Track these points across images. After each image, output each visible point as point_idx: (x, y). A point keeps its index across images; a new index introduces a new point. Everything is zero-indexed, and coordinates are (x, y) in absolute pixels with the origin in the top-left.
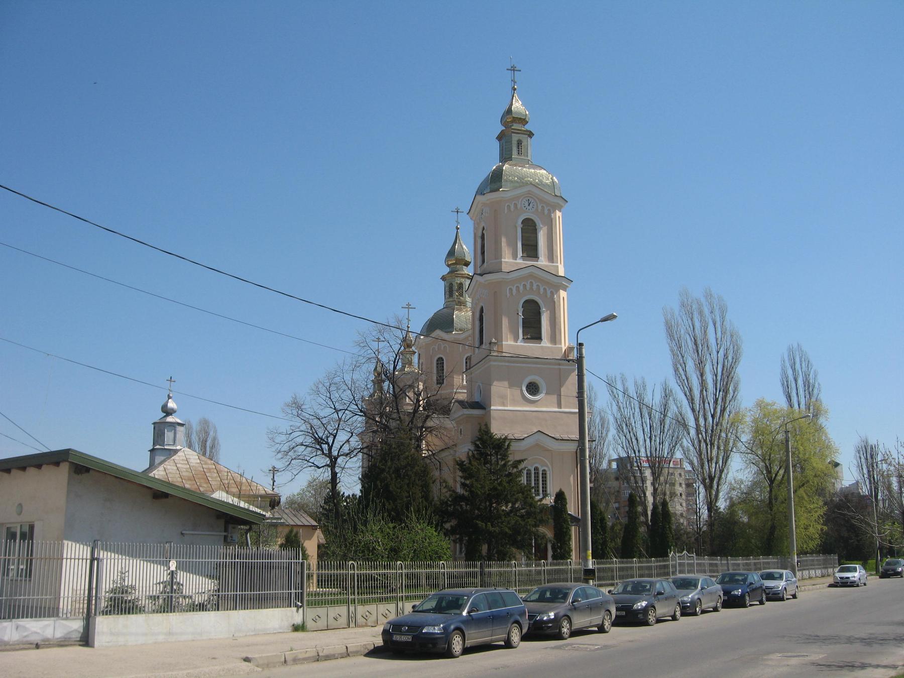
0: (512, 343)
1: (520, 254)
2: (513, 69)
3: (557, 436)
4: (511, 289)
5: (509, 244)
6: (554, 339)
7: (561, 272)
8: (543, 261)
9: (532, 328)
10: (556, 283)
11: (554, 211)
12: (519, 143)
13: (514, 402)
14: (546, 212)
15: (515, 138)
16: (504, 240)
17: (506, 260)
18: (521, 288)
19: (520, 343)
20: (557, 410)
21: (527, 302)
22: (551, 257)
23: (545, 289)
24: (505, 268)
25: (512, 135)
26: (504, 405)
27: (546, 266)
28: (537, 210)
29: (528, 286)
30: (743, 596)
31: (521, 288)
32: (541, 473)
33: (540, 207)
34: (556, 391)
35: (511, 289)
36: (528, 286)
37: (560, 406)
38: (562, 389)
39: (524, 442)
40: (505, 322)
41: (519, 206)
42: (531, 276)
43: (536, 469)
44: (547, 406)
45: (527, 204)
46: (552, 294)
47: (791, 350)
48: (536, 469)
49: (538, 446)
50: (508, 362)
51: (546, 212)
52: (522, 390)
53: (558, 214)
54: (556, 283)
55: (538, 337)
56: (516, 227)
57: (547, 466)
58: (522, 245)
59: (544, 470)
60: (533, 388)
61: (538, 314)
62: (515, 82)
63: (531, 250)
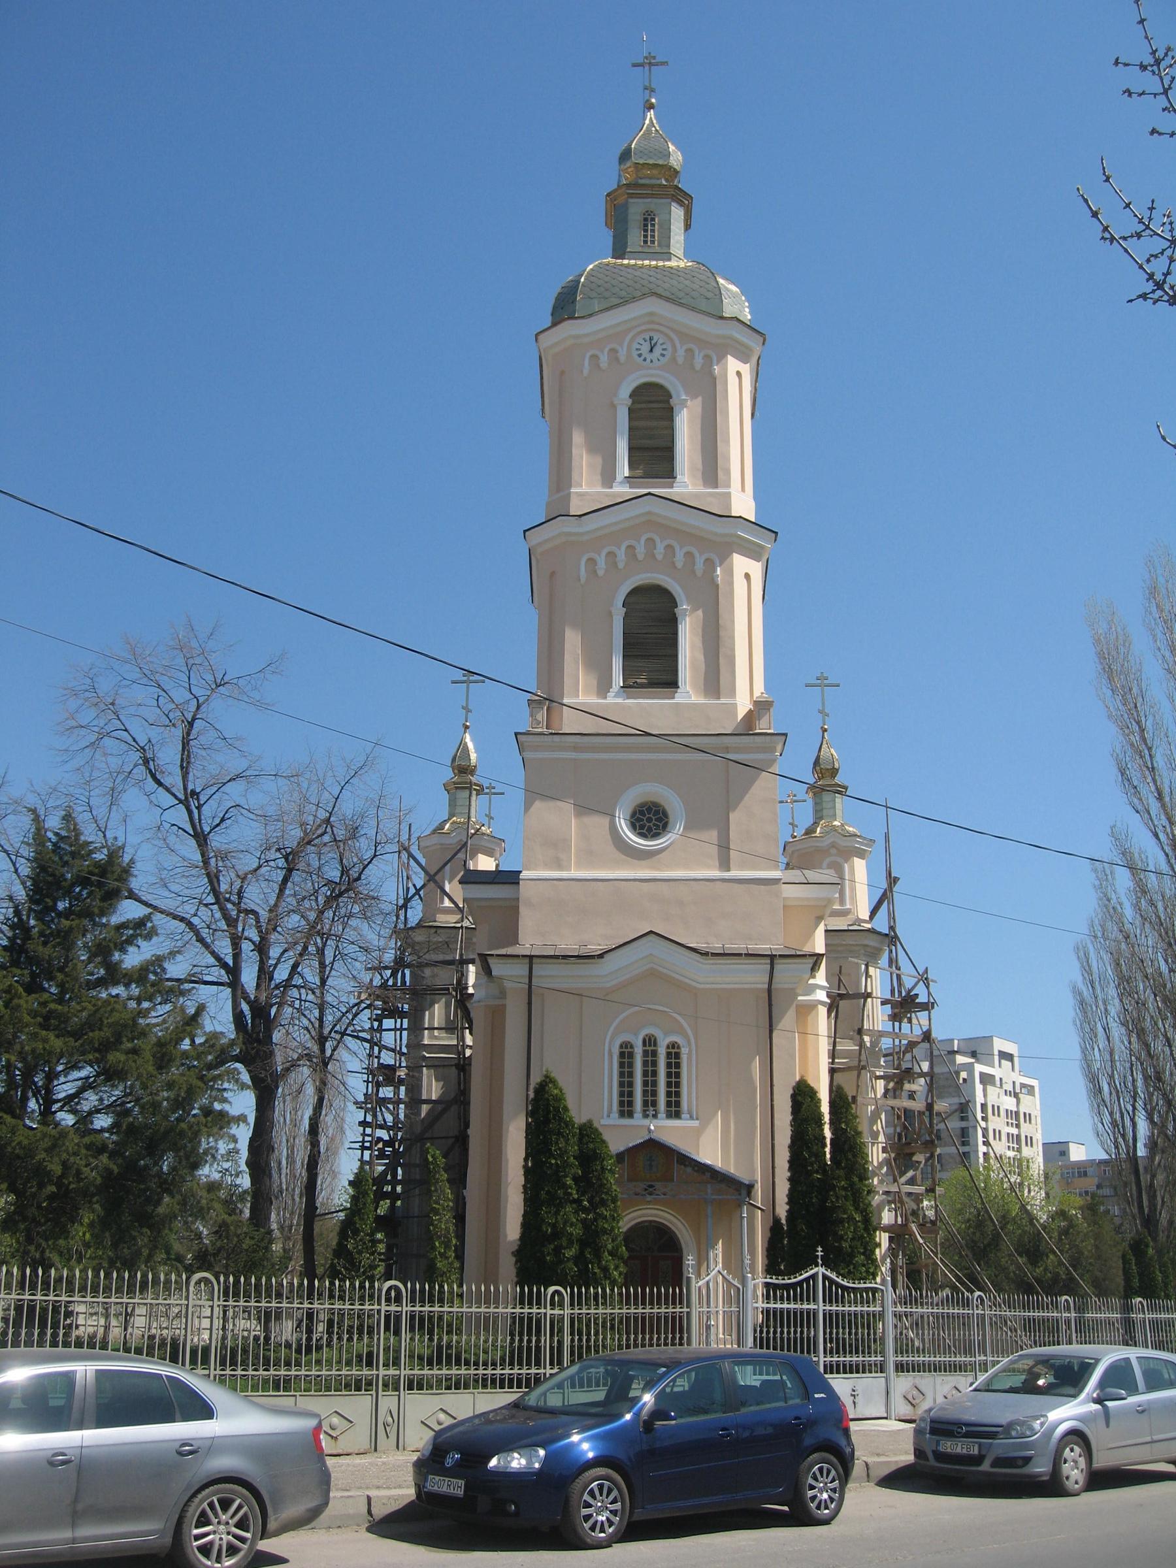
0: (594, 696)
1: (624, 469)
2: (650, 63)
3: (716, 946)
4: (591, 561)
5: (592, 449)
6: (715, 679)
7: (743, 504)
8: (687, 483)
9: (649, 652)
11: (721, 358)
12: (648, 219)
13: (589, 857)
14: (698, 361)
15: (636, 209)
16: (578, 438)
17: (584, 489)
18: (621, 554)
19: (614, 699)
20: (716, 873)
21: (635, 592)
22: (712, 469)
23: (689, 555)
26: (560, 866)
27: (697, 496)
28: (674, 359)
29: (641, 551)
30: (558, 1480)
31: (621, 554)
33: (681, 352)
34: (714, 817)
35: (591, 561)
36: (641, 551)
37: (725, 864)
38: (733, 817)
40: (572, 640)
41: (622, 354)
42: (650, 523)
43: (650, 1041)
44: (686, 866)
45: (646, 347)
46: (710, 565)
48: (650, 1041)
49: (654, 976)
50: (576, 748)
51: (698, 361)
52: (613, 830)
53: (733, 364)
54: (718, 536)
55: (669, 682)
56: (613, 407)
57: (681, 1031)
58: (631, 449)
59: (673, 1045)
60: (651, 819)
61: (672, 623)
62: (653, 91)
63: (653, 455)
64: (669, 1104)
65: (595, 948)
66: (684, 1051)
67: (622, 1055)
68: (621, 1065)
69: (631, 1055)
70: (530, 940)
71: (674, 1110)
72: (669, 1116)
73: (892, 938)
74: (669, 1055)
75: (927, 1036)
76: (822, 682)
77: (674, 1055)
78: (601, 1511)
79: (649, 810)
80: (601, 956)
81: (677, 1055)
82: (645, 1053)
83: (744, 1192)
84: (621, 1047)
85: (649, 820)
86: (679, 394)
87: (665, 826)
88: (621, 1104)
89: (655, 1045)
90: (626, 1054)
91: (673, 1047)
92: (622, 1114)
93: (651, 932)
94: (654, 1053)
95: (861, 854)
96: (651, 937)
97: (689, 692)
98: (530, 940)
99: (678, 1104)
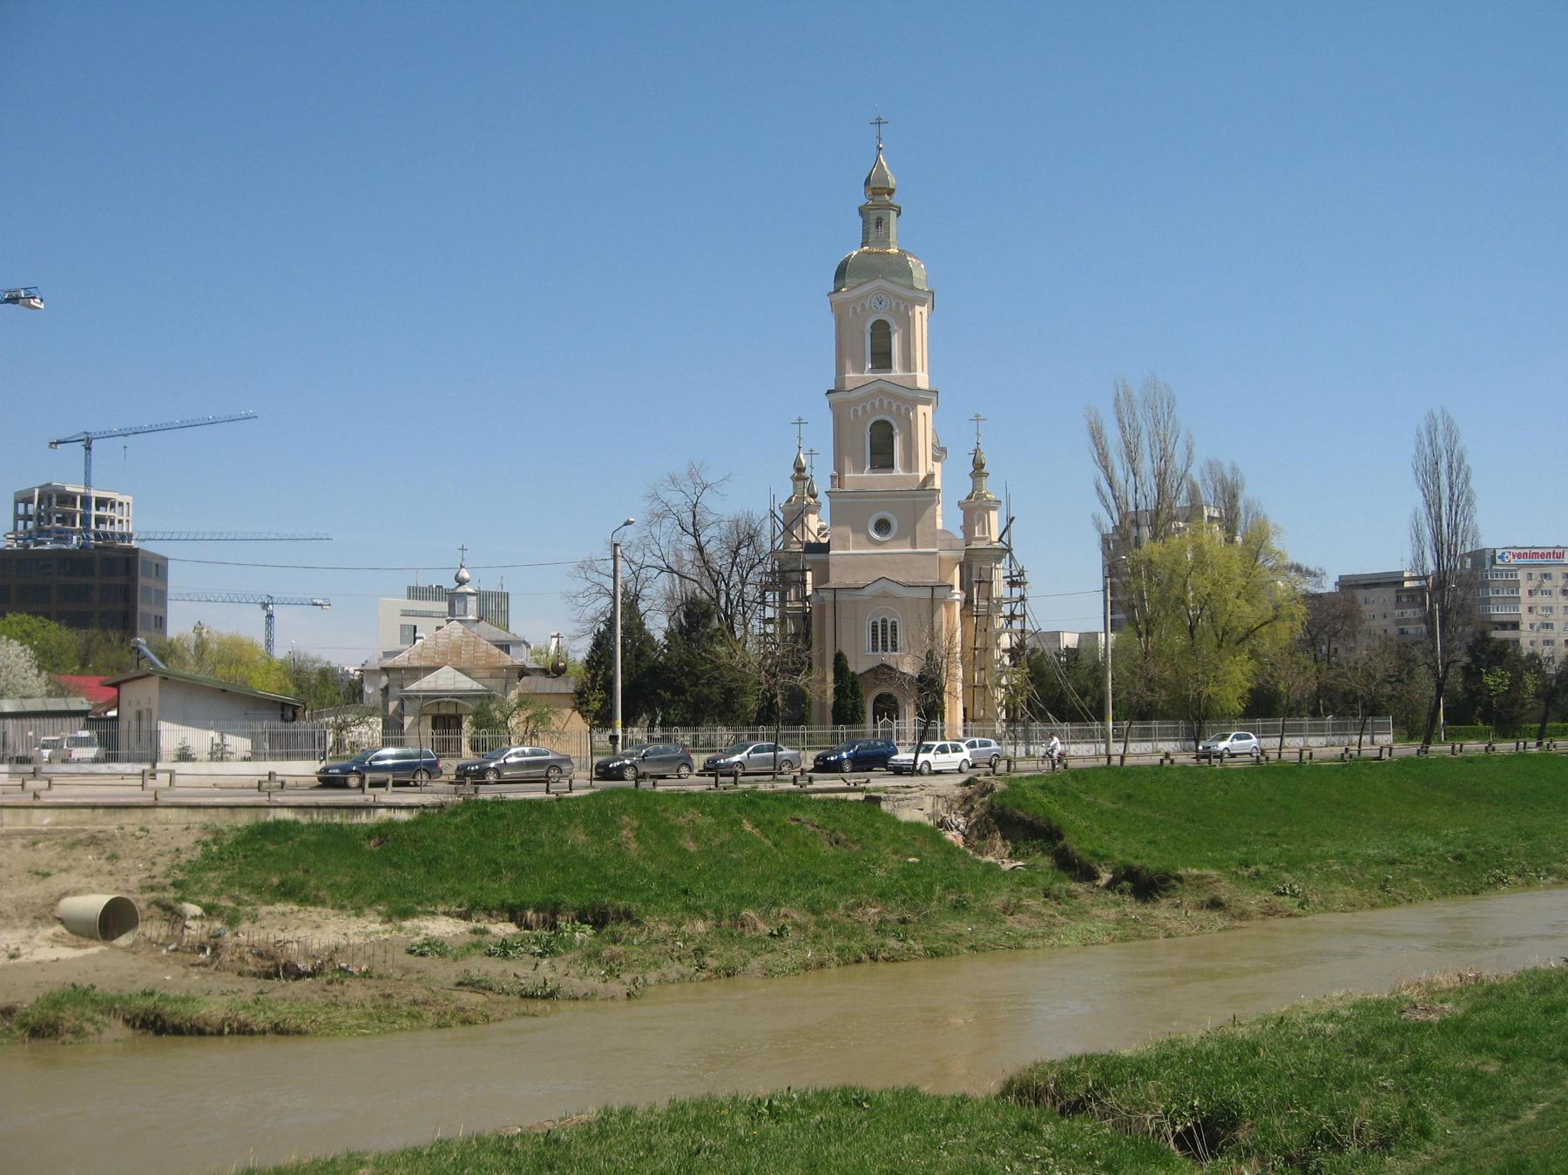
6: (910, 464)
7: (923, 380)
8: (897, 371)
9: (882, 456)
10: (911, 398)
13: (857, 545)
19: (866, 474)
22: (908, 364)
23: (898, 407)
24: (848, 386)
25: (878, 205)
37: (914, 545)
39: (867, 591)
42: (881, 391)
43: (884, 621)
47: (1431, 417)
48: (884, 621)
49: (885, 595)
54: (911, 398)
55: (891, 466)
63: (882, 359)
65: (862, 583)
70: (834, 581)
73: (1009, 550)
75: (1022, 598)
76: (977, 418)
78: (847, 767)
86: (894, 326)
90: (875, 626)
95: (995, 509)
97: (898, 470)
98: (834, 581)
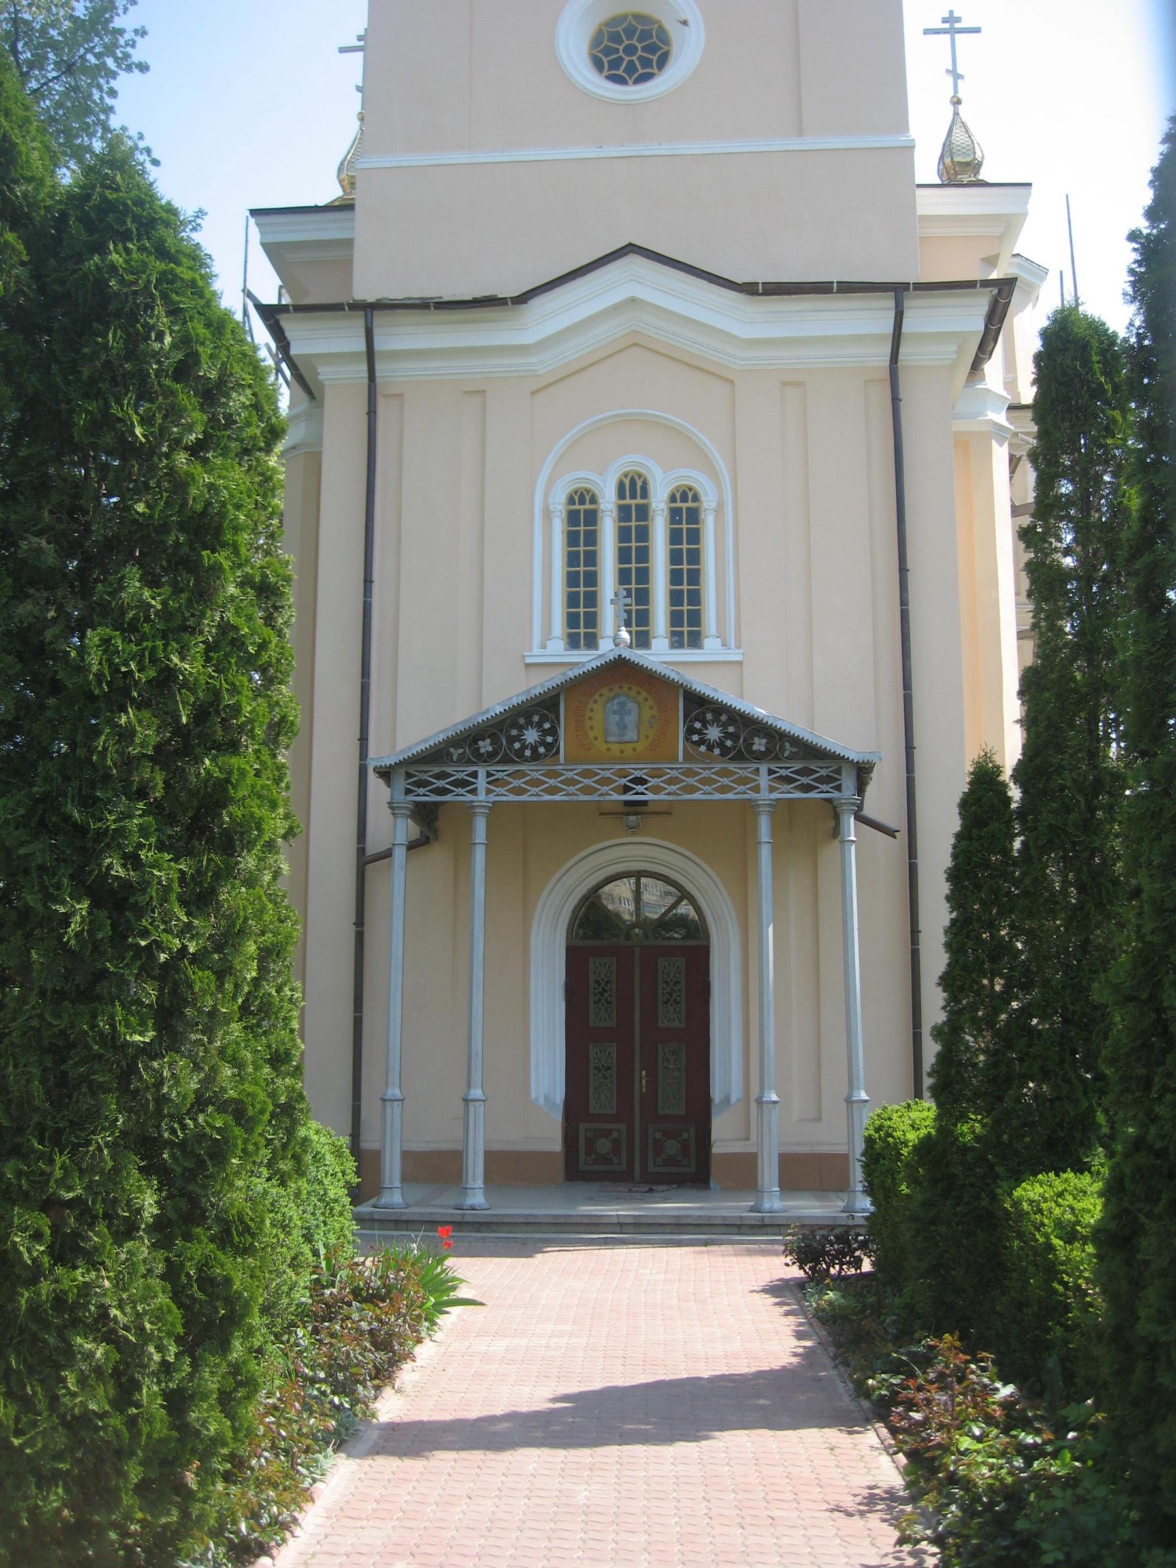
32: (659, 503)
43: (633, 488)
48: (633, 488)
64: (675, 619)
66: (708, 502)
67: (573, 518)
68: (572, 539)
69: (592, 518)
71: (687, 627)
72: (677, 641)
74: (675, 514)
77: (686, 513)
79: (630, 32)
80: (523, 299)
81: (694, 516)
82: (624, 512)
83: (848, 782)
84: (571, 501)
85: (630, 50)
87: (663, 61)
88: (572, 620)
89: (645, 493)
90: (581, 517)
91: (684, 498)
92: (573, 642)
93: (631, 249)
94: (643, 512)
96: (634, 262)
99: (695, 618)
